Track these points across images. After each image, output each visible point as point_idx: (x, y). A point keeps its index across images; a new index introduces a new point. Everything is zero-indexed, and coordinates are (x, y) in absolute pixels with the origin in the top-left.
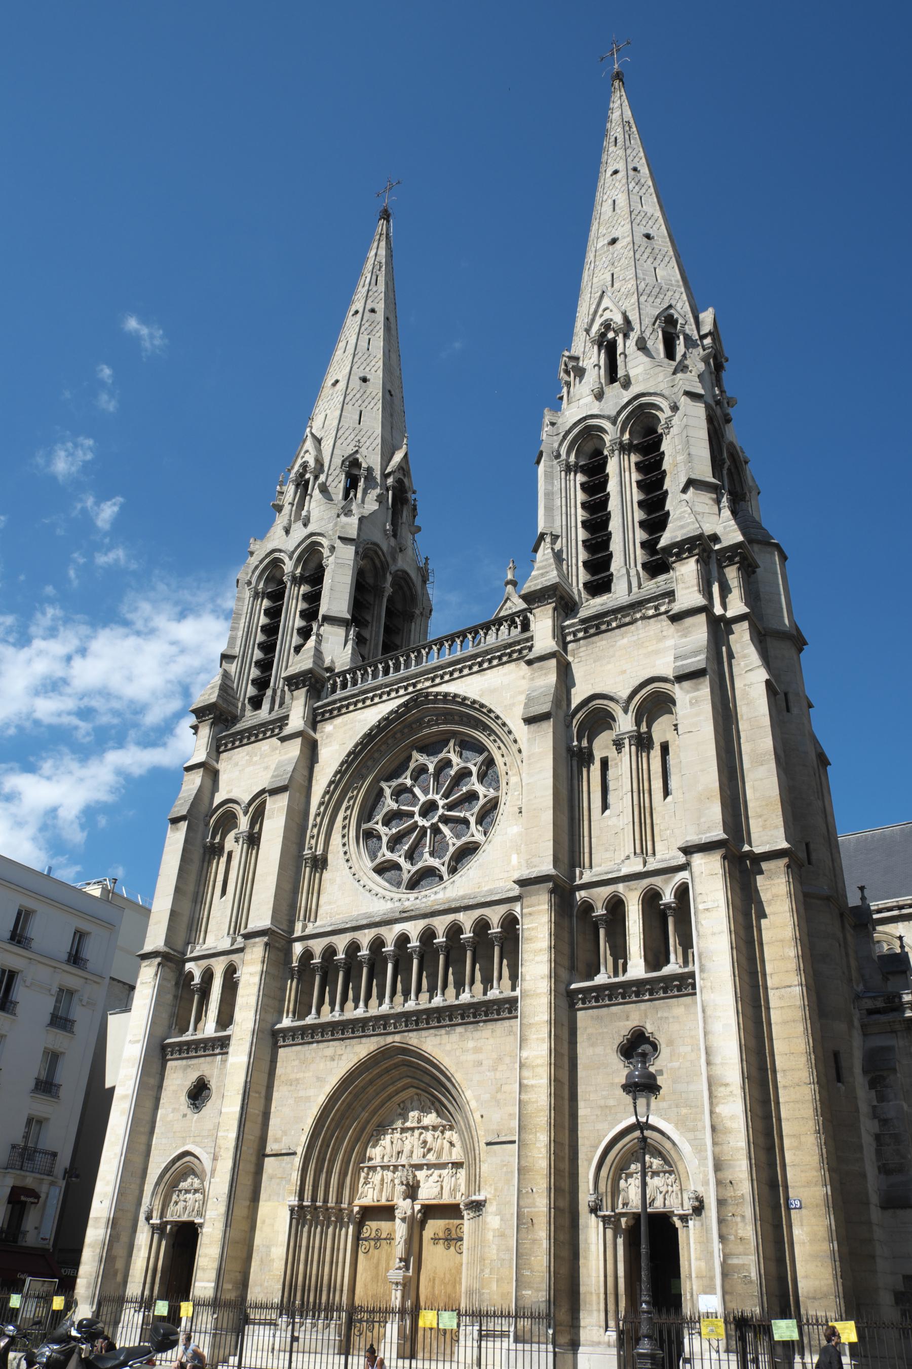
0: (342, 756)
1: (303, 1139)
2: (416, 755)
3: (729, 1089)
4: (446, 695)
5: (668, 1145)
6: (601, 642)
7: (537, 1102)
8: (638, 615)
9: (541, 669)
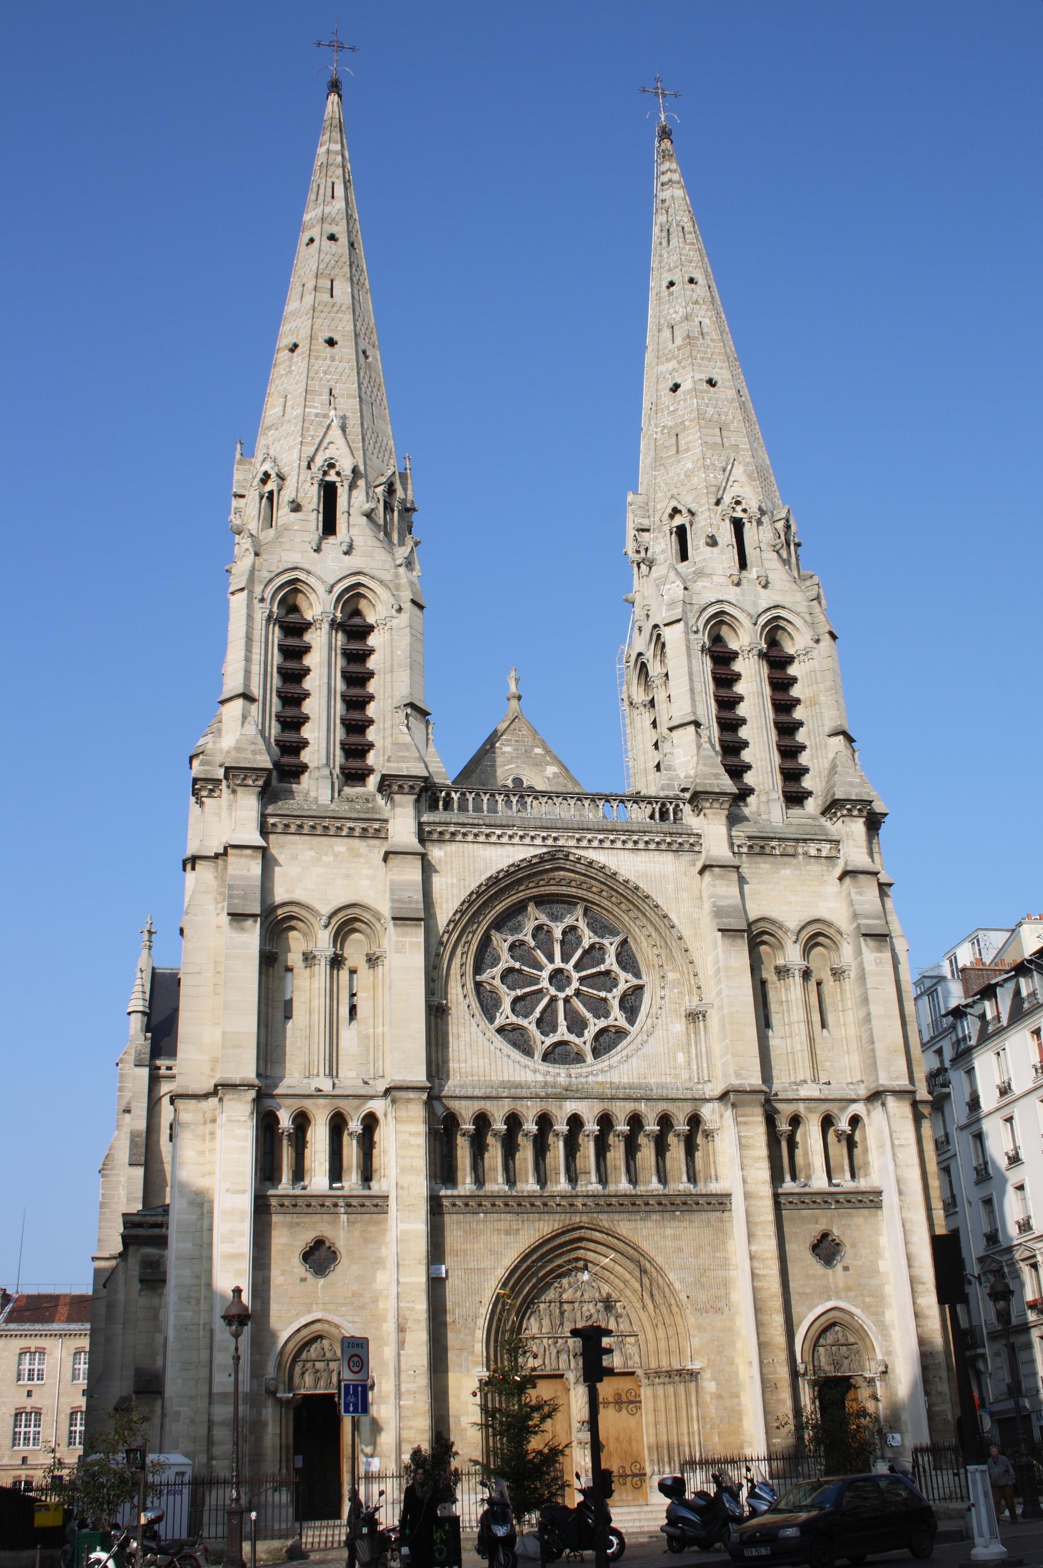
0: (464, 895)
3: (925, 1286)
4: (590, 864)
7: (769, 1289)
9: (721, 877)
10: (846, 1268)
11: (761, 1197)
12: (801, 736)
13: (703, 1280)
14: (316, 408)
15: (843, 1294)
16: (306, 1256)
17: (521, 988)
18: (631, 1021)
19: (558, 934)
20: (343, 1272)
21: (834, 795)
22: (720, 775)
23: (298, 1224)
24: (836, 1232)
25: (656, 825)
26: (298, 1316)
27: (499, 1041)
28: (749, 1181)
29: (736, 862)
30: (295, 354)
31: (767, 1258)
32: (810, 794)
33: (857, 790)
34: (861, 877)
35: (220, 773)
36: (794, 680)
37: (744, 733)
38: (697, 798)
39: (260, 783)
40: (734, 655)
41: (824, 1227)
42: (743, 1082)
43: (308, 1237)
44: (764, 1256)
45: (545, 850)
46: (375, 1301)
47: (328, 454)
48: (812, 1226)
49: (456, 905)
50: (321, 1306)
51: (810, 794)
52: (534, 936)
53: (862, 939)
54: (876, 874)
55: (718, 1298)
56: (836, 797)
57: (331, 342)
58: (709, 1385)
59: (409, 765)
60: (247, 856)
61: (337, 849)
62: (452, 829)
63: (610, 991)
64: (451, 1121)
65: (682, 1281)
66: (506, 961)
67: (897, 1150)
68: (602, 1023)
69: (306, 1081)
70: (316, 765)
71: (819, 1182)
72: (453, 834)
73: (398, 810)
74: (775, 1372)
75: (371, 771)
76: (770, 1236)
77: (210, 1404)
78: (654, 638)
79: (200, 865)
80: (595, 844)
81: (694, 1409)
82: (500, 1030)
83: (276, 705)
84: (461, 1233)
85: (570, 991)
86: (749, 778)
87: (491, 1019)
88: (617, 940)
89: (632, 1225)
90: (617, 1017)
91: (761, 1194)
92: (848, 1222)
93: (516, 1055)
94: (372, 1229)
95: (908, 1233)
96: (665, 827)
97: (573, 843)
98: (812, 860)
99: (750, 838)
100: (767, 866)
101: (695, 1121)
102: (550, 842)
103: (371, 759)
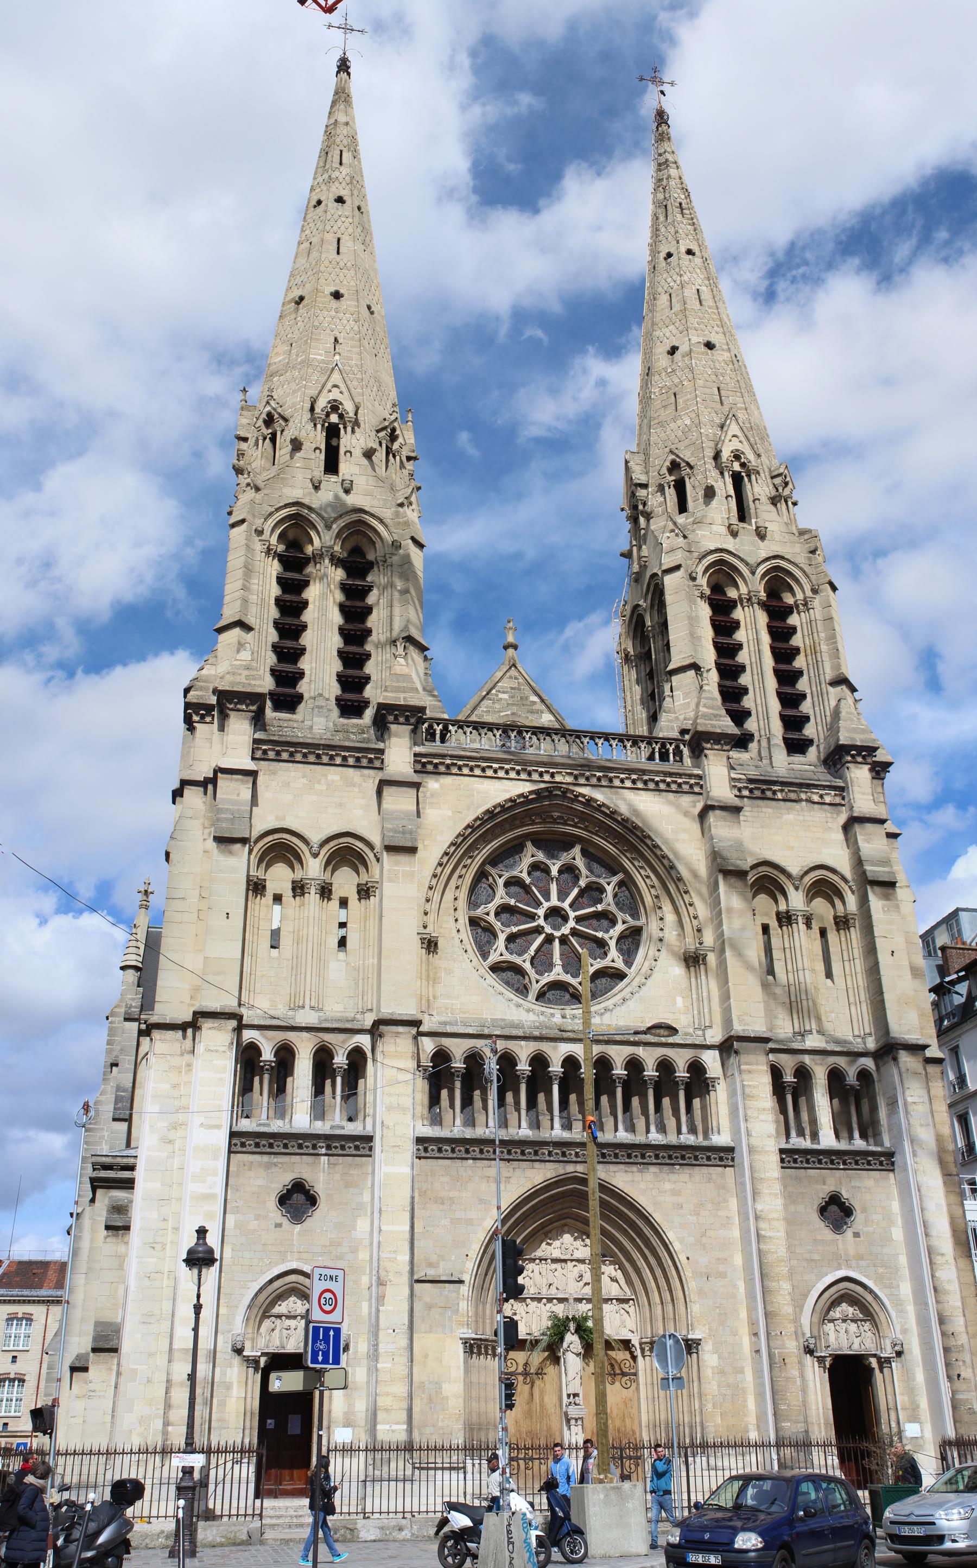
0: (459, 828)
1: (470, 1265)
2: (530, 848)
3: (945, 1258)
4: (589, 802)
5: (869, 1298)
6: (767, 810)
8: (803, 796)
10: (856, 1235)
11: (766, 1152)
12: (802, 685)
13: (704, 1240)
14: (321, 355)
15: (853, 1263)
16: (283, 1200)
17: (516, 925)
18: (629, 963)
19: (554, 871)
20: (320, 1218)
21: (838, 740)
22: (721, 716)
23: (275, 1165)
24: (845, 1194)
25: (657, 765)
26: (271, 1265)
27: (491, 979)
28: (754, 1134)
29: (737, 802)
30: (301, 306)
31: (773, 1219)
32: (811, 742)
33: (862, 736)
34: (868, 825)
35: (213, 700)
36: (793, 630)
37: (744, 680)
38: (699, 741)
39: (254, 708)
40: (732, 604)
41: (833, 1189)
42: (746, 1028)
43: (284, 1179)
44: (770, 1217)
45: (543, 786)
46: (355, 1251)
47: (331, 396)
48: (819, 1187)
49: (450, 837)
50: (296, 1256)
51: (811, 742)
52: (529, 874)
53: (868, 887)
54: (882, 822)
55: (721, 1261)
56: (841, 742)
57: (337, 295)
58: (709, 1357)
59: (407, 695)
60: (237, 780)
61: (330, 777)
62: (448, 762)
63: (607, 931)
64: (441, 1056)
65: (681, 1240)
66: (501, 896)
67: (910, 1108)
68: (598, 964)
69: (291, 1013)
70: (312, 694)
71: (828, 1139)
72: (448, 767)
73: (394, 740)
74: (783, 1346)
75: (366, 703)
76: (776, 1194)
77: (170, 1361)
78: (652, 588)
79: (188, 791)
80: (594, 781)
81: (696, 1384)
82: (495, 968)
83: (273, 636)
84: (446, 1179)
85: (566, 930)
86: (751, 725)
87: (485, 956)
88: (615, 879)
89: (628, 1177)
90: (614, 958)
91: (767, 1149)
92: (858, 1184)
93: (509, 994)
94: (354, 1172)
95: (925, 1199)
96: (666, 767)
97: (569, 779)
98: (816, 806)
99: (751, 781)
100: (770, 810)
101: (696, 1068)
102: (547, 777)
103: (368, 691)
